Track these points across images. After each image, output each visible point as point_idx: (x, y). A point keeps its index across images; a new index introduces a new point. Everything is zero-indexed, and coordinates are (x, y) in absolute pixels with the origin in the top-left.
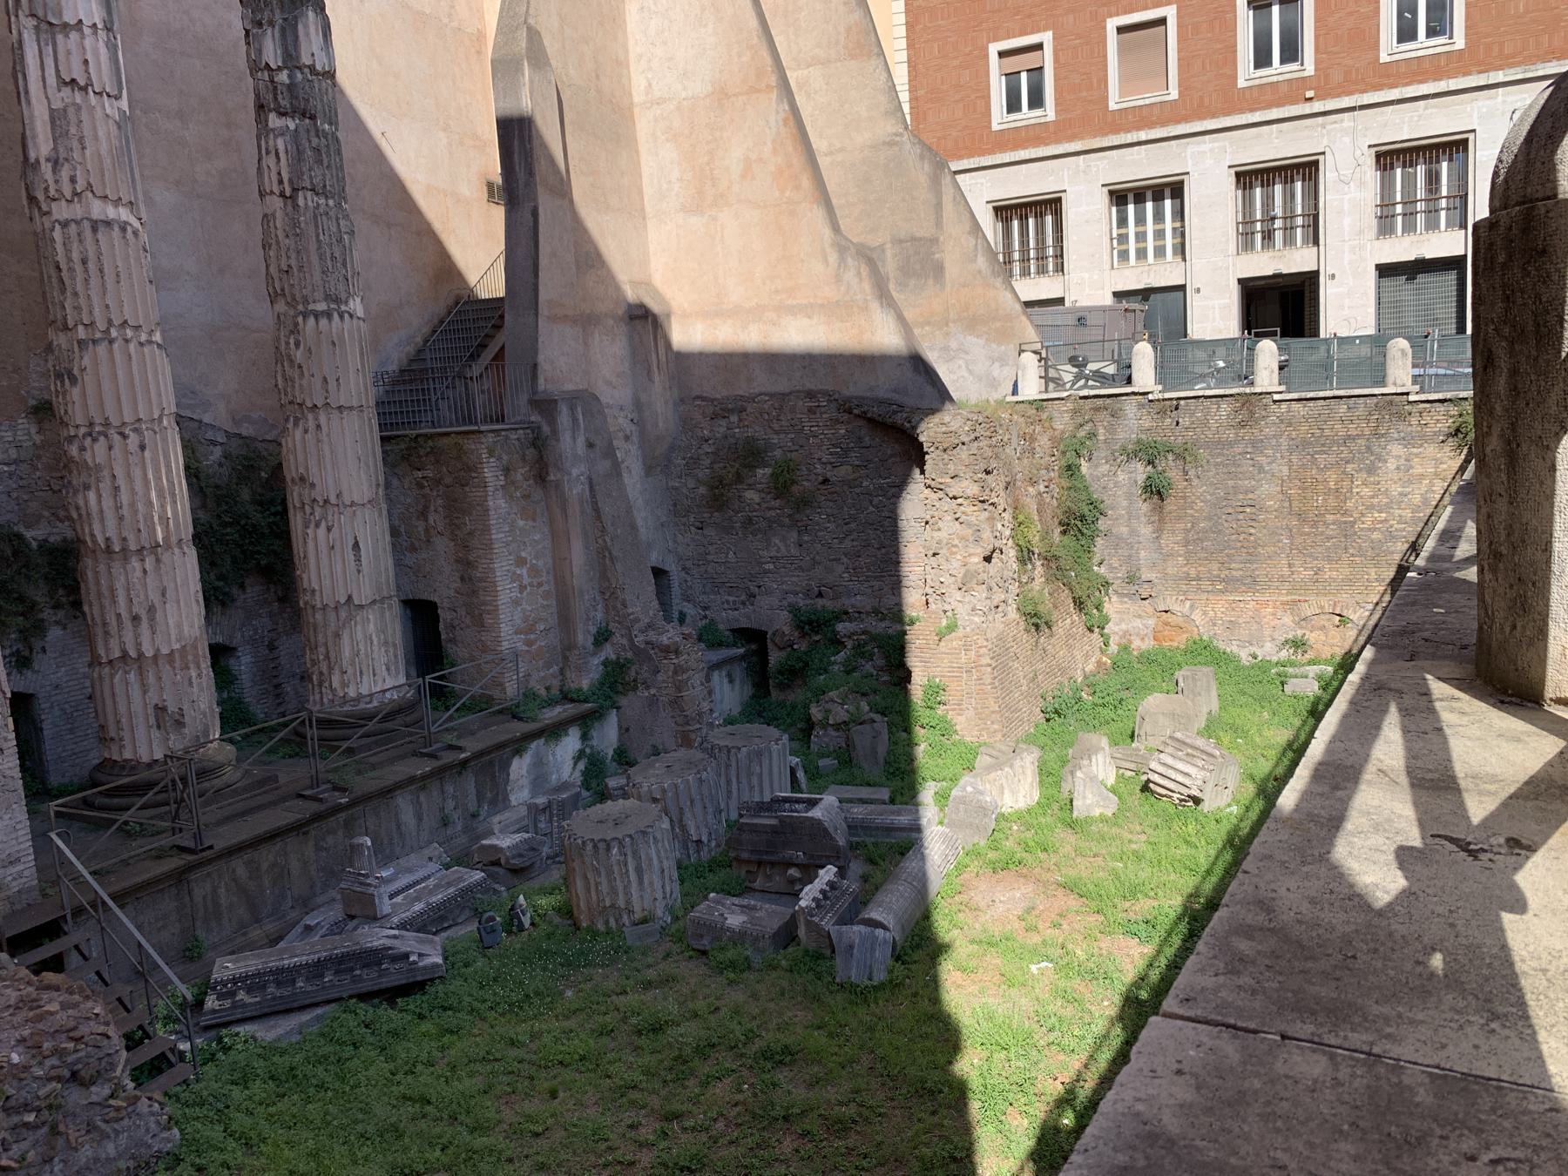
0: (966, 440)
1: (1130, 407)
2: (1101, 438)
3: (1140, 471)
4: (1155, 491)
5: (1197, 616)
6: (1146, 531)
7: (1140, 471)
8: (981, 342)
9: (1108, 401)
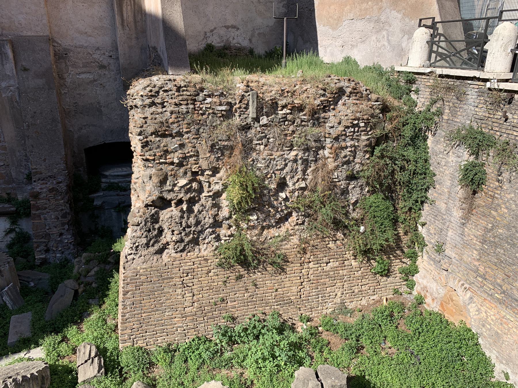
0: (139, 103)
1: (472, 92)
2: (445, 117)
3: (465, 156)
4: (473, 180)
5: (472, 308)
6: (457, 214)
7: (465, 156)
8: (400, 16)
9: (458, 82)
